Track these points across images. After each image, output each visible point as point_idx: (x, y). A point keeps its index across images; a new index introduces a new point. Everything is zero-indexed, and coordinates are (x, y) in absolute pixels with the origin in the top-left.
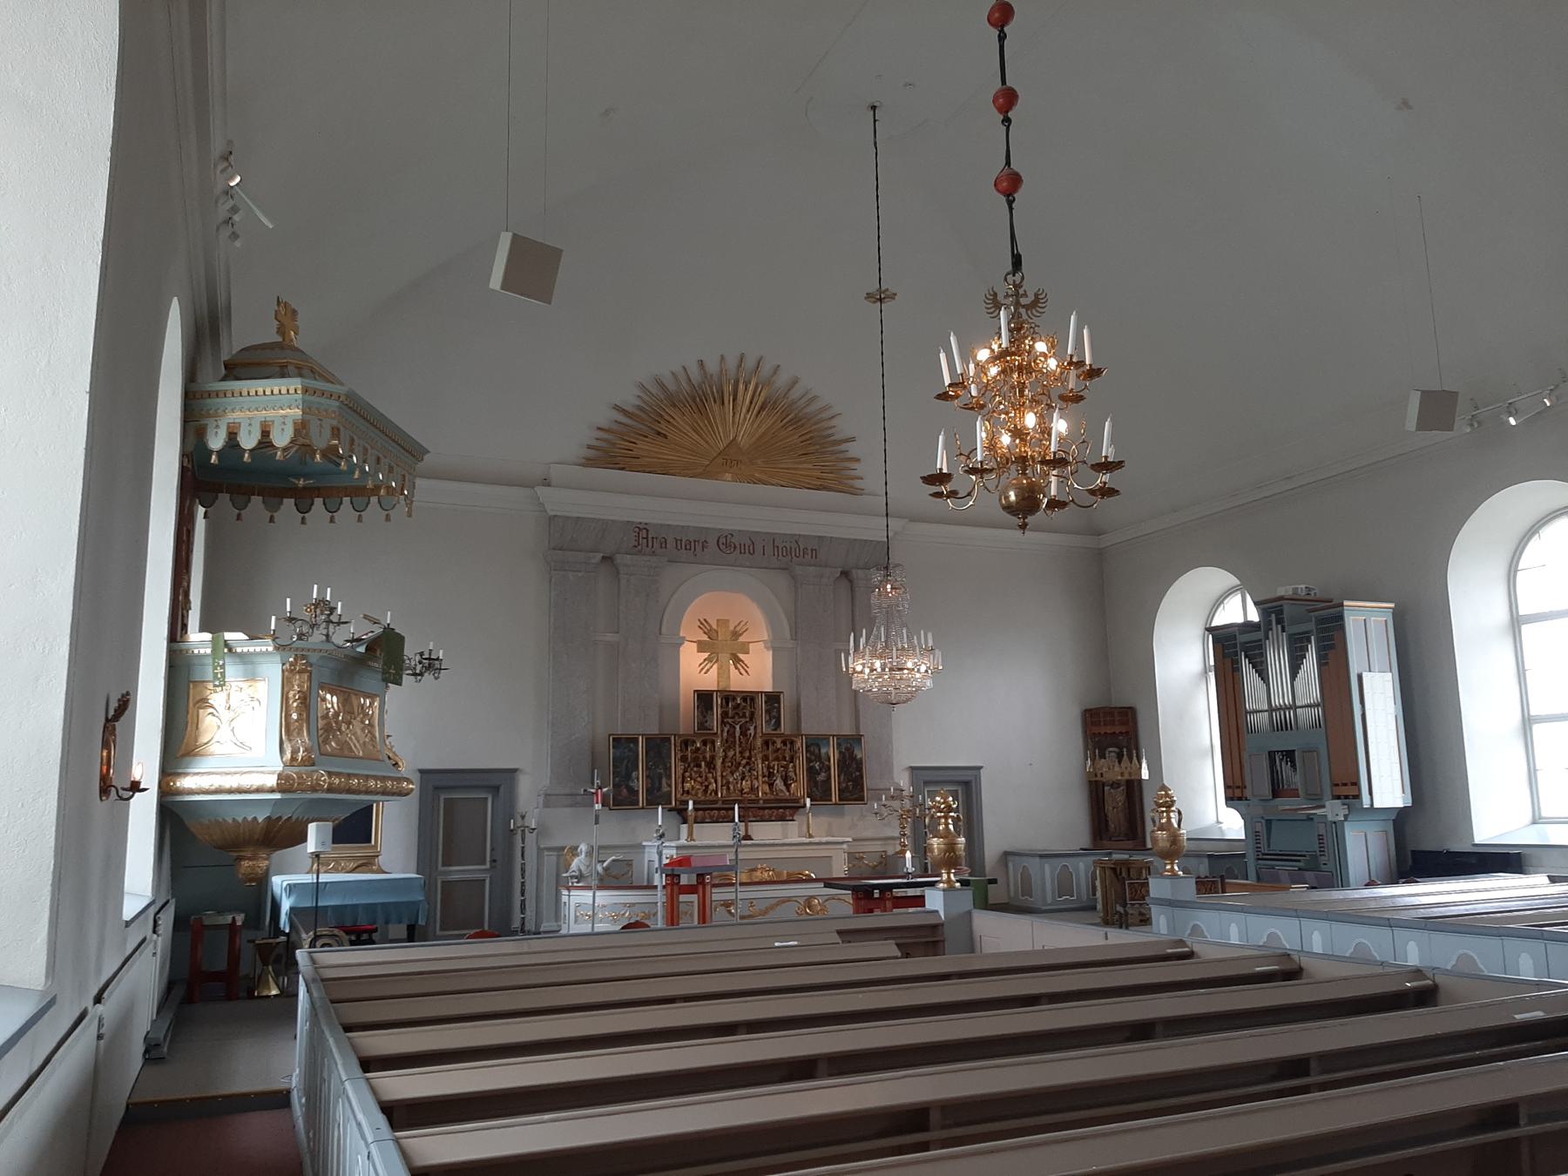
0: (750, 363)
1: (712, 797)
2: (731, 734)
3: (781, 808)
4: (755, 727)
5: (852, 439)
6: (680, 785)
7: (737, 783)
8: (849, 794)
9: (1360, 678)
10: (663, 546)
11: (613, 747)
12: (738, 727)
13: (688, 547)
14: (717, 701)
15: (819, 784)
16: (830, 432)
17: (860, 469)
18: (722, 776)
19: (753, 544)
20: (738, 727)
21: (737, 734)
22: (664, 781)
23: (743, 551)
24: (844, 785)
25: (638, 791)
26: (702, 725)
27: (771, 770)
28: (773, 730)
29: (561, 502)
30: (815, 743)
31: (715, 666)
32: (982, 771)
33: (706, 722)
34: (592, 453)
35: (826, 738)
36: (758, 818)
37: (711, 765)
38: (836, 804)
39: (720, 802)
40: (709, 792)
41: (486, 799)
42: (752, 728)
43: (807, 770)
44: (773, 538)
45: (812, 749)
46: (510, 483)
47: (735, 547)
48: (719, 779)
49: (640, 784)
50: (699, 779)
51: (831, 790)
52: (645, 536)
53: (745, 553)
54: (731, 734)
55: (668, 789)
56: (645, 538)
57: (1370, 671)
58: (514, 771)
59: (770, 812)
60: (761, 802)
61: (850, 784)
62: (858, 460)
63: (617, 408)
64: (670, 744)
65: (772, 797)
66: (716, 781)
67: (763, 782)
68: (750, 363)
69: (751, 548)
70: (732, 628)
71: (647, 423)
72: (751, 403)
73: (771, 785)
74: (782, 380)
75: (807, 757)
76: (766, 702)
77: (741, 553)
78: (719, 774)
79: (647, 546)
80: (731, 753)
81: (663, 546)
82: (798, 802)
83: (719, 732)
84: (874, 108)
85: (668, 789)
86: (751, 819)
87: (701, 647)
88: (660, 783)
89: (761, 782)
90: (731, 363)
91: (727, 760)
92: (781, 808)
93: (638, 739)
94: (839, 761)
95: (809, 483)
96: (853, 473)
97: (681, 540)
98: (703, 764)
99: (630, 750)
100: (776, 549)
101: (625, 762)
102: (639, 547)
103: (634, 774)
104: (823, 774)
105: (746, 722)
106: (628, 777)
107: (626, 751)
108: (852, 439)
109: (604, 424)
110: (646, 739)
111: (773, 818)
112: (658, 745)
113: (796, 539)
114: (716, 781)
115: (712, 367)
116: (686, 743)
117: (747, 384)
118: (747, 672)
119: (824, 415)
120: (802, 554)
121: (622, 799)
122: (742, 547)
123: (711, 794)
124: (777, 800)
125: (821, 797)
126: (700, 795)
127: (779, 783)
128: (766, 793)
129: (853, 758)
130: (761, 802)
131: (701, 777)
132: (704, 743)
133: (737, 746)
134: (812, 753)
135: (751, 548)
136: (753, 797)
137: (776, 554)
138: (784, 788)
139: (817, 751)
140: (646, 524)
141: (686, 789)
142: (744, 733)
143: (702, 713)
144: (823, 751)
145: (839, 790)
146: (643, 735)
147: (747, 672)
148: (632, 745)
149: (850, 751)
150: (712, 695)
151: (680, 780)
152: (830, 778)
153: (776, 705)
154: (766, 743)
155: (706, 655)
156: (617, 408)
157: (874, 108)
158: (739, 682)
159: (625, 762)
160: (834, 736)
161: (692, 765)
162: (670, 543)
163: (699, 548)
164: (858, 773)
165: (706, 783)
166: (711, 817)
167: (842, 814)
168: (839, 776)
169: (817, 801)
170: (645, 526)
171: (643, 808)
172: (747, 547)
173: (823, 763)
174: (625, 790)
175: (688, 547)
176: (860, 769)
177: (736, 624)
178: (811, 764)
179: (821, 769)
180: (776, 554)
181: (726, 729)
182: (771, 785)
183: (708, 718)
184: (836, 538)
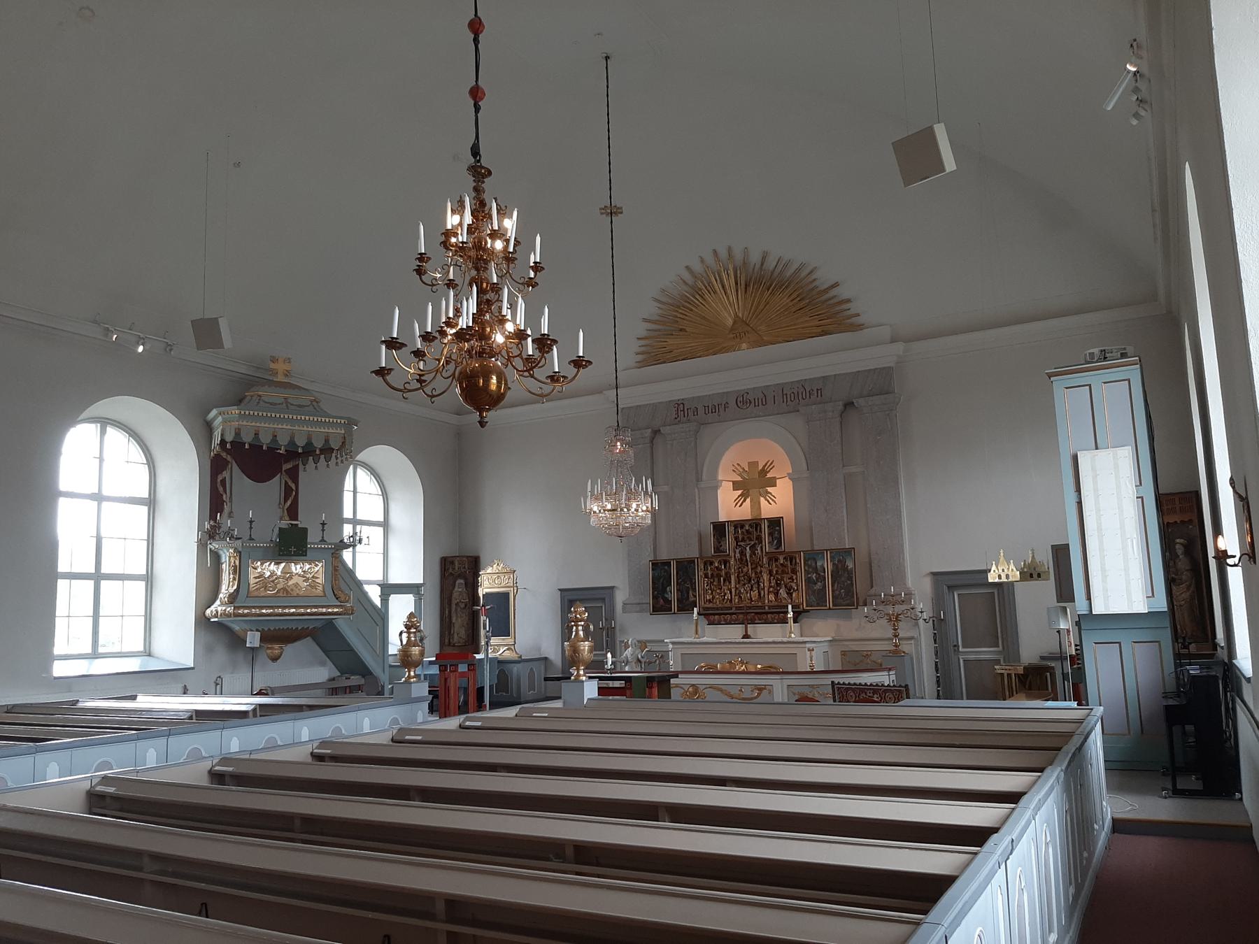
0: (723, 254)
1: (728, 604)
2: (743, 553)
3: (717, 614)
4: (762, 547)
5: (836, 285)
7: (747, 593)
9: (1075, 459)
10: (696, 413)
11: (653, 570)
12: (748, 548)
13: (714, 411)
14: (730, 531)
16: (814, 284)
17: (854, 308)
18: (736, 588)
19: (765, 396)
20: (748, 548)
21: (748, 555)
22: (691, 592)
23: (757, 404)
24: (837, 593)
25: (671, 601)
26: (717, 550)
28: (776, 549)
29: (629, 397)
30: (812, 556)
31: (748, 500)
32: (615, 589)
33: (721, 546)
34: (640, 357)
35: (821, 553)
36: (763, 621)
37: (728, 579)
38: (830, 609)
39: (734, 609)
41: (602, 607)
42: (759, 548)
43: (805, 580)
44: (782, 387)
45: (809, 563)
46: (592, 393)
47: (750, 402)
48: (733, 590)
49: (673, 594)
50: (718, 591)
52: (682, 409)
53: (758, 406)
54: (743, 553)
56: (682, 410)
57: (1097, 448)
58: (612, 588)
59: (773, 616)
60: (767, 608)
61: (843, 591)
62: (848, 301)
63: (645, 320)
64: (695, 564)
65: (776, 603)
66: (731, 593)
67: (769, 592)
68: (723, 254)
69: (764, 400)
70: (760, 468)
71: (668, 324)
72: (736, 284)
73: (776, 594)
74: (755, 258)
75: (805, 570)
76: (768, 527)
77: (755, 406)
79: (684, 416)
80: (745, 570)
81: (696, 413)
82: (799, 608)
83: (732, 554)
84: (607, 58)
86: (756, 622)
87: (736, 486)
88: (688, 596)
89: (766, 593)
90: (710, 260)
91: (742, 575)
92: (717, 614)
93: (670, 562)
94: (832, 572)
95: (809, 333)
96: (849, 313)
97: (708, 407)
99: (666, 571)
100: (785, 396)
101: (661, 580)
102: (679, 419)
103: (668, 588)
104: (819, 584)
105: (755, 544)
106: (664, 591)
107: (662, 571)
108: (836, 285)
109: (643, 333)
110: (677, 562)
111: (776, 621)
112: (686, 566)
113: (802, 384)
114: (731, 593)
115: (698, 268)
116: (708, 563)
117: (726, 270)
118: (775, 502)
119: (804, 274)
120: (808, 394)
121: (660, 606)
122: (756, 400)
123: (726, 602)
124: (780, 606)
125: (818, 604)
126: (718, 602)
127: (783, 592)
128: (771, 601)
129: (845, 569)
130: (767, 608)
132: (720, 563)
133: (749, 564)
134: (810, 566)
135: (764, 400)
136: (760, 604)
137: (785, 400)
138: (785, 596)
139: (814, 564)
140: (683, 400)
141: (708, 598)
142: (753, 553)
143: (717, 539)
144: (819, 564)
147: (775, 502)
148: (666, 567)
149: (843, 562)
150: (725, 524)
153: (777, 528)
154: (770, 560)
155: (740, 492)
156: (645, 320)
157: (607, 58)
158: (768, 510)
159: (661, 580)
160: (827, 550)
162: (701, 411)
163: (722, 410)
164: (849, 582)
166: (725, 620)
167: (849, 617)
168: (832, 586)
170: (682, 402)
171: (674, 613)
172: (760, 400)
173: (819, 574)
174: (662, 601)
175: (714, 411)
176: (850, 578)
177: (764, 464)
179: (817, 579)
180: (785, 400)
181: (737, 551)
182: (776, 594)
183: (722, 543)
184: (839, 375)
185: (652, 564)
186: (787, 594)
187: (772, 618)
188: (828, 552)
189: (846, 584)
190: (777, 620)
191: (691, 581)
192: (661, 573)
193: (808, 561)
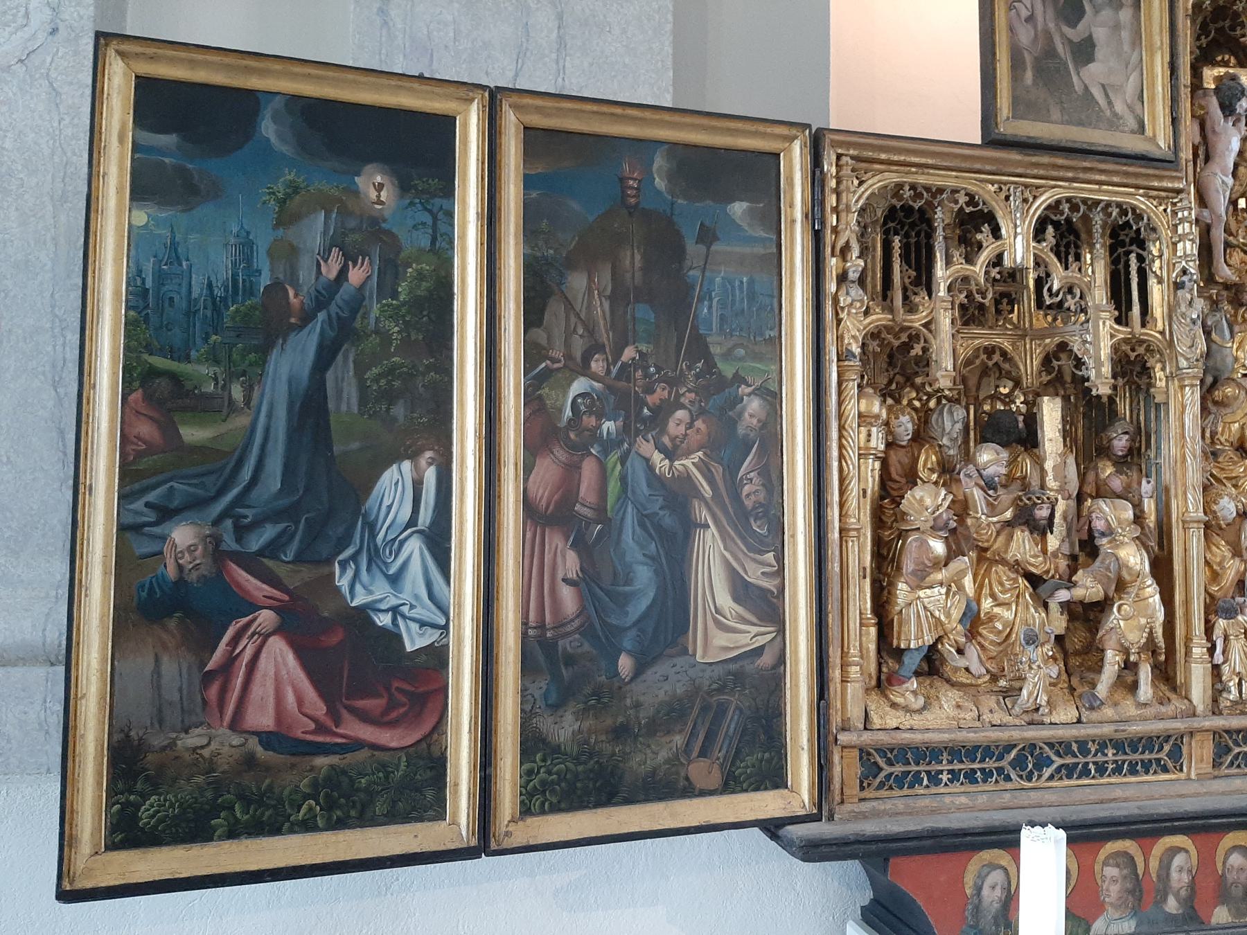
6: (861, 597)
25: (437, 657)
33: (1085, 51)
39: (1200, 753)
40: (1112, 659)
50: (1022, 546)
55: (751, 636)
64: (773, 219)
66: (1162, 569)
78: (1188, 505)
85: (751, 636)
98: (1051, 413)
110: (534, 138)
126: (1034, 689)
131: (1041, 530)
146: (495, 98)
151: (860, 554)
161: (951, 422)
165: (1088, 587)
185: (146, 88)
191: (727, 415)
192: (287, 254)
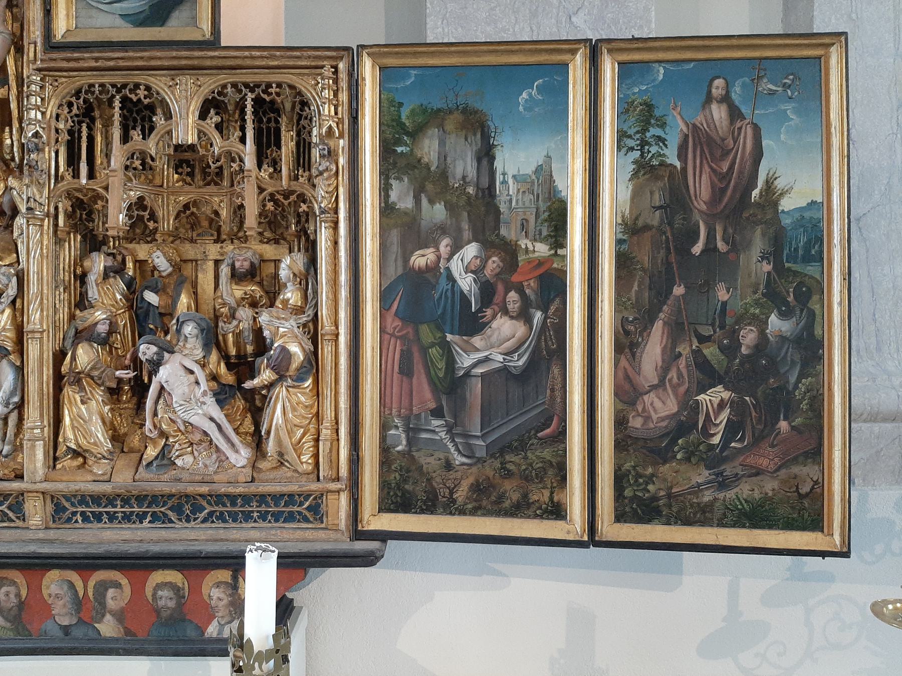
8: (701, 475)
15: (477, 387)
27: (151, 297)
43: (385, 297)
51: (561, 435)
75: (387, 209)
111: (108, 628)
125: (480, 489)
145: (621, 444)
152: (560, 353)
160: (594, 51)
164: (776, 324)
169: (451, 508)
173: (510, 252)
178: (421, 259)
179: (487, 292)
186: (222, 395)
187: (78, 603)
188: (609, 69)
189: (748, 337)
190: (120, 616)
193: (416, 133)
